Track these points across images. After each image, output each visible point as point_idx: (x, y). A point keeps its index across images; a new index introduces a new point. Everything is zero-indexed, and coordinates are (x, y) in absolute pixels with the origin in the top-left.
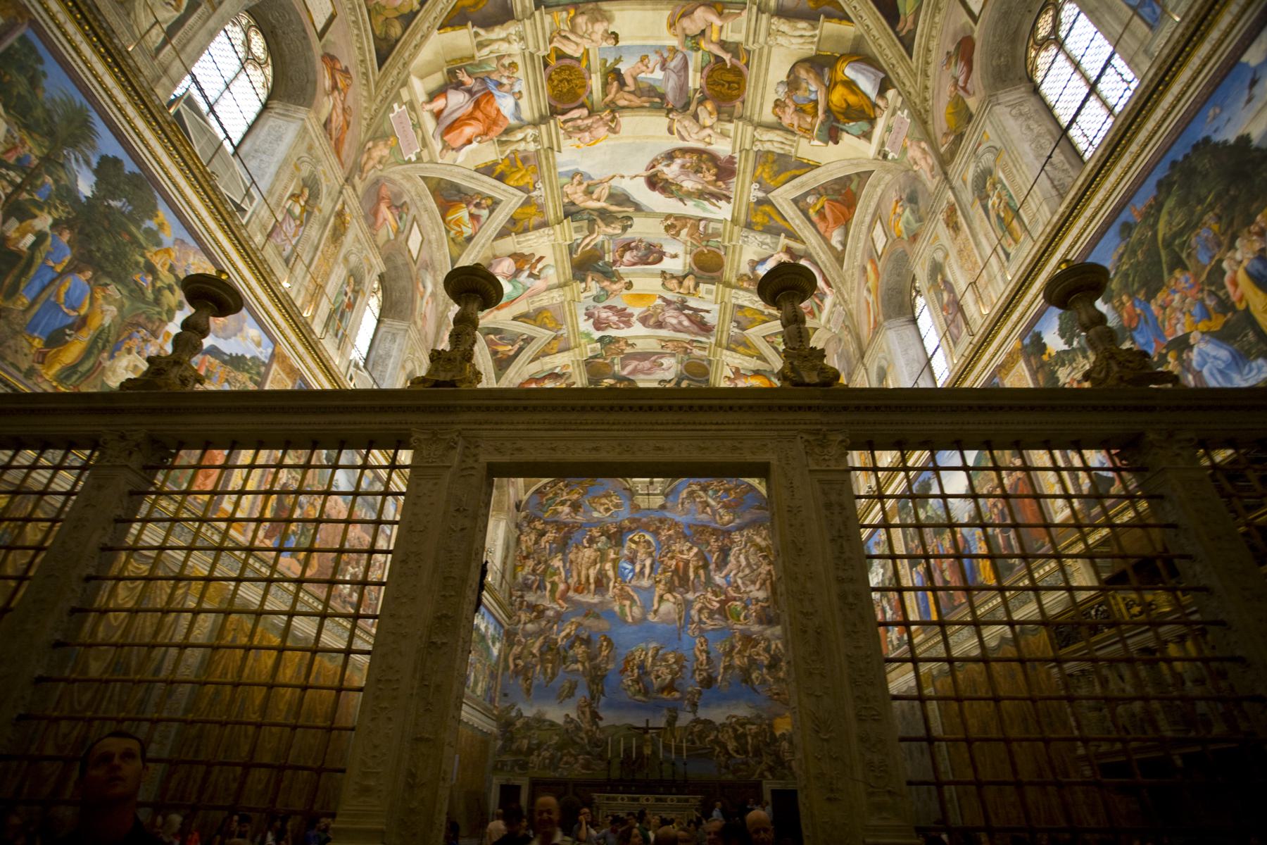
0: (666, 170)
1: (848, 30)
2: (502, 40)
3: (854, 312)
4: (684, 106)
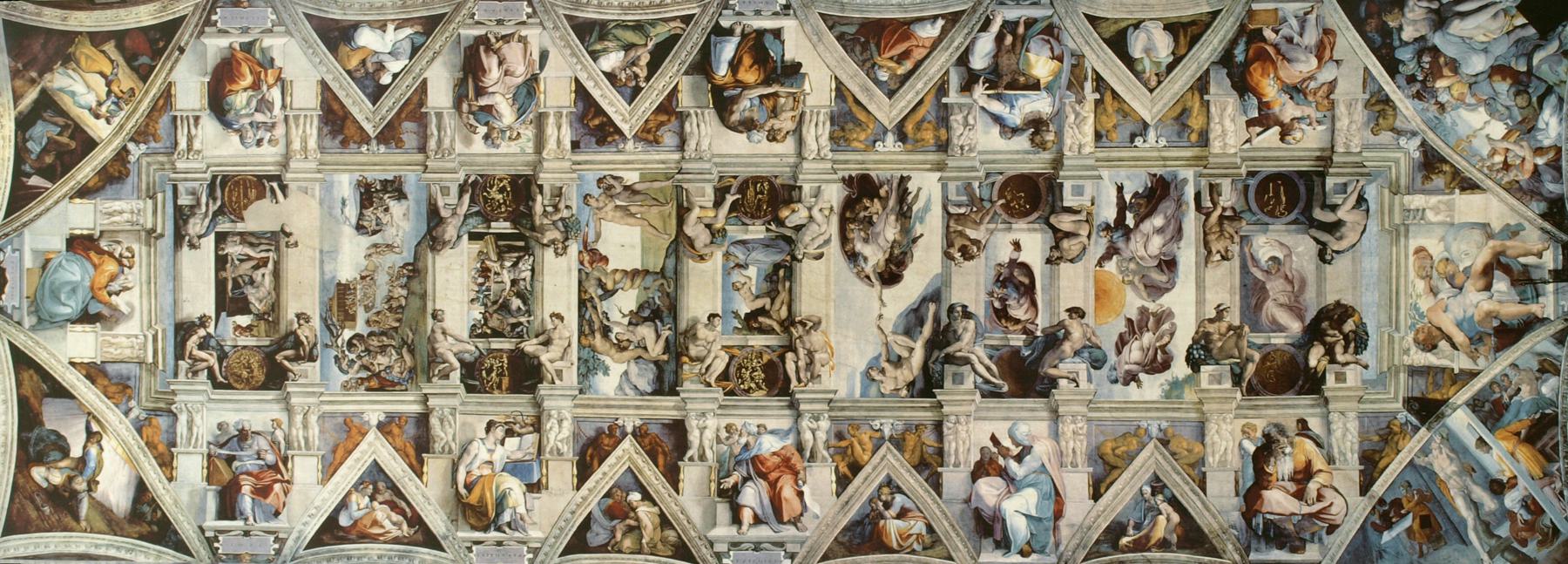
0: (871, 262)
1: (685, 83)
4: (787, 241)
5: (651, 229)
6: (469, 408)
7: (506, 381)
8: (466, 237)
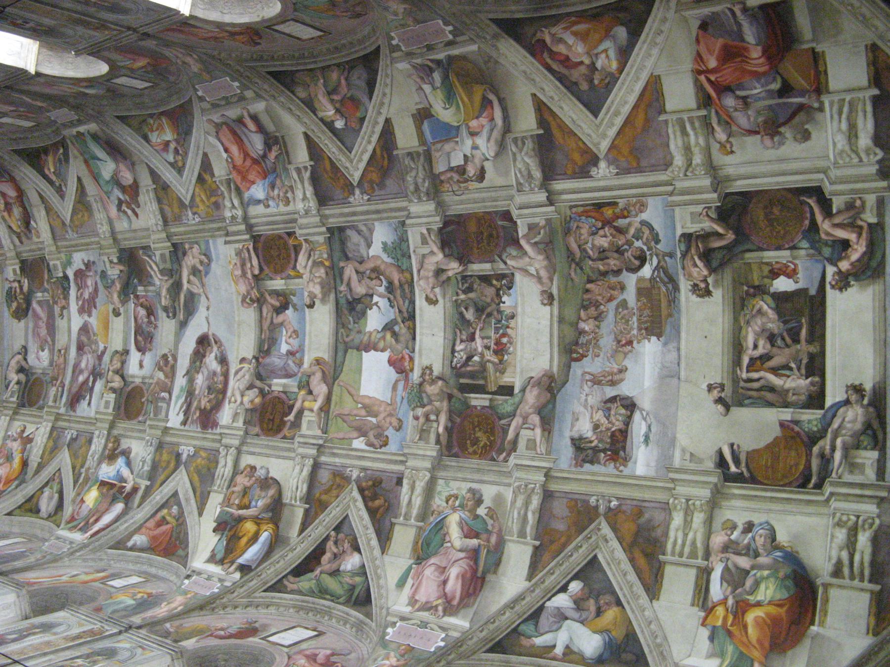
0: (213, 355)
2: (304, 194)
3: (59, 564)
5: (353, 392)
6: (504, 193)
7: (472, 227)
8: (516, 390)
